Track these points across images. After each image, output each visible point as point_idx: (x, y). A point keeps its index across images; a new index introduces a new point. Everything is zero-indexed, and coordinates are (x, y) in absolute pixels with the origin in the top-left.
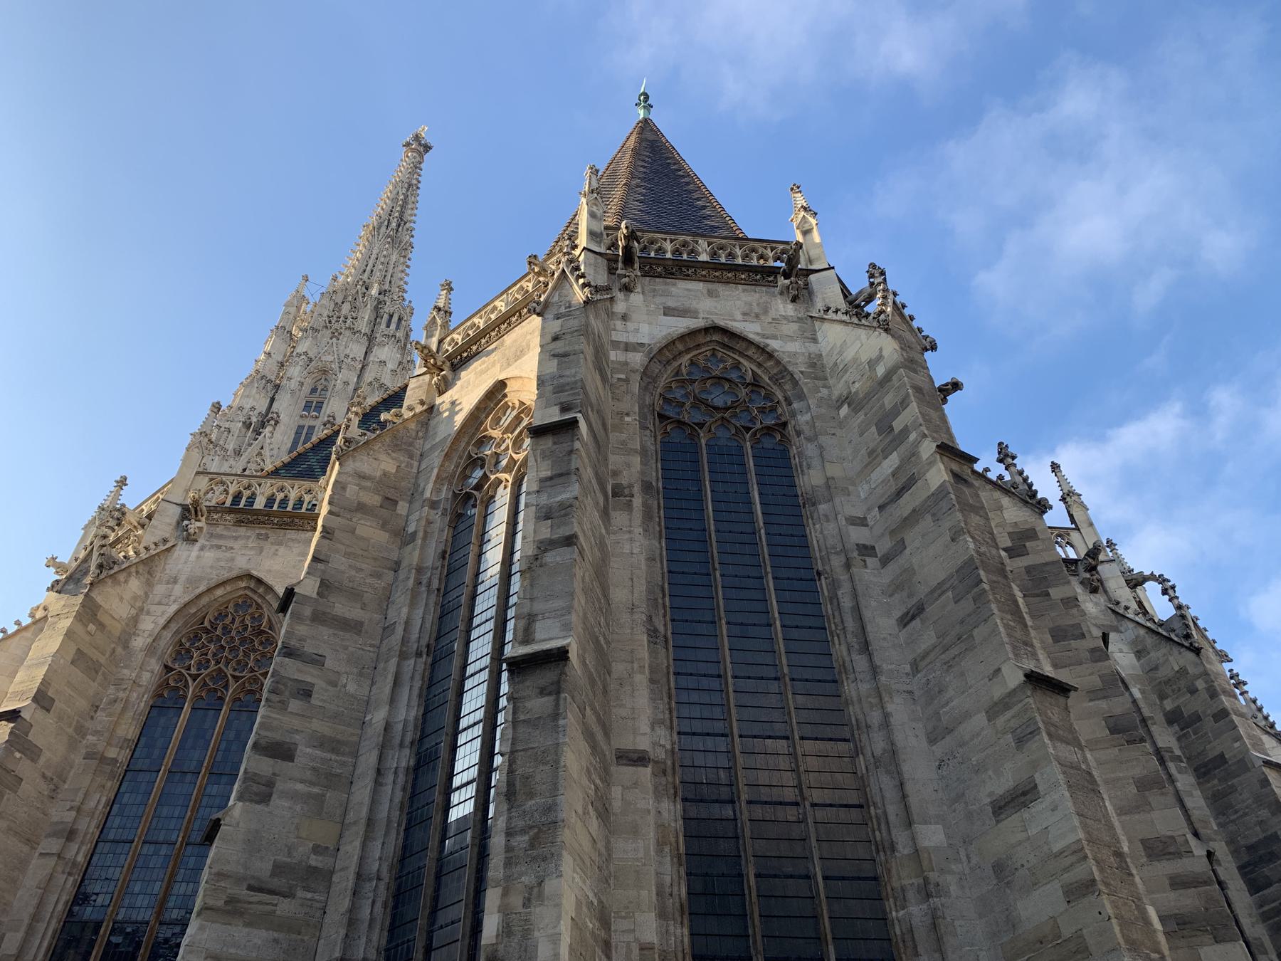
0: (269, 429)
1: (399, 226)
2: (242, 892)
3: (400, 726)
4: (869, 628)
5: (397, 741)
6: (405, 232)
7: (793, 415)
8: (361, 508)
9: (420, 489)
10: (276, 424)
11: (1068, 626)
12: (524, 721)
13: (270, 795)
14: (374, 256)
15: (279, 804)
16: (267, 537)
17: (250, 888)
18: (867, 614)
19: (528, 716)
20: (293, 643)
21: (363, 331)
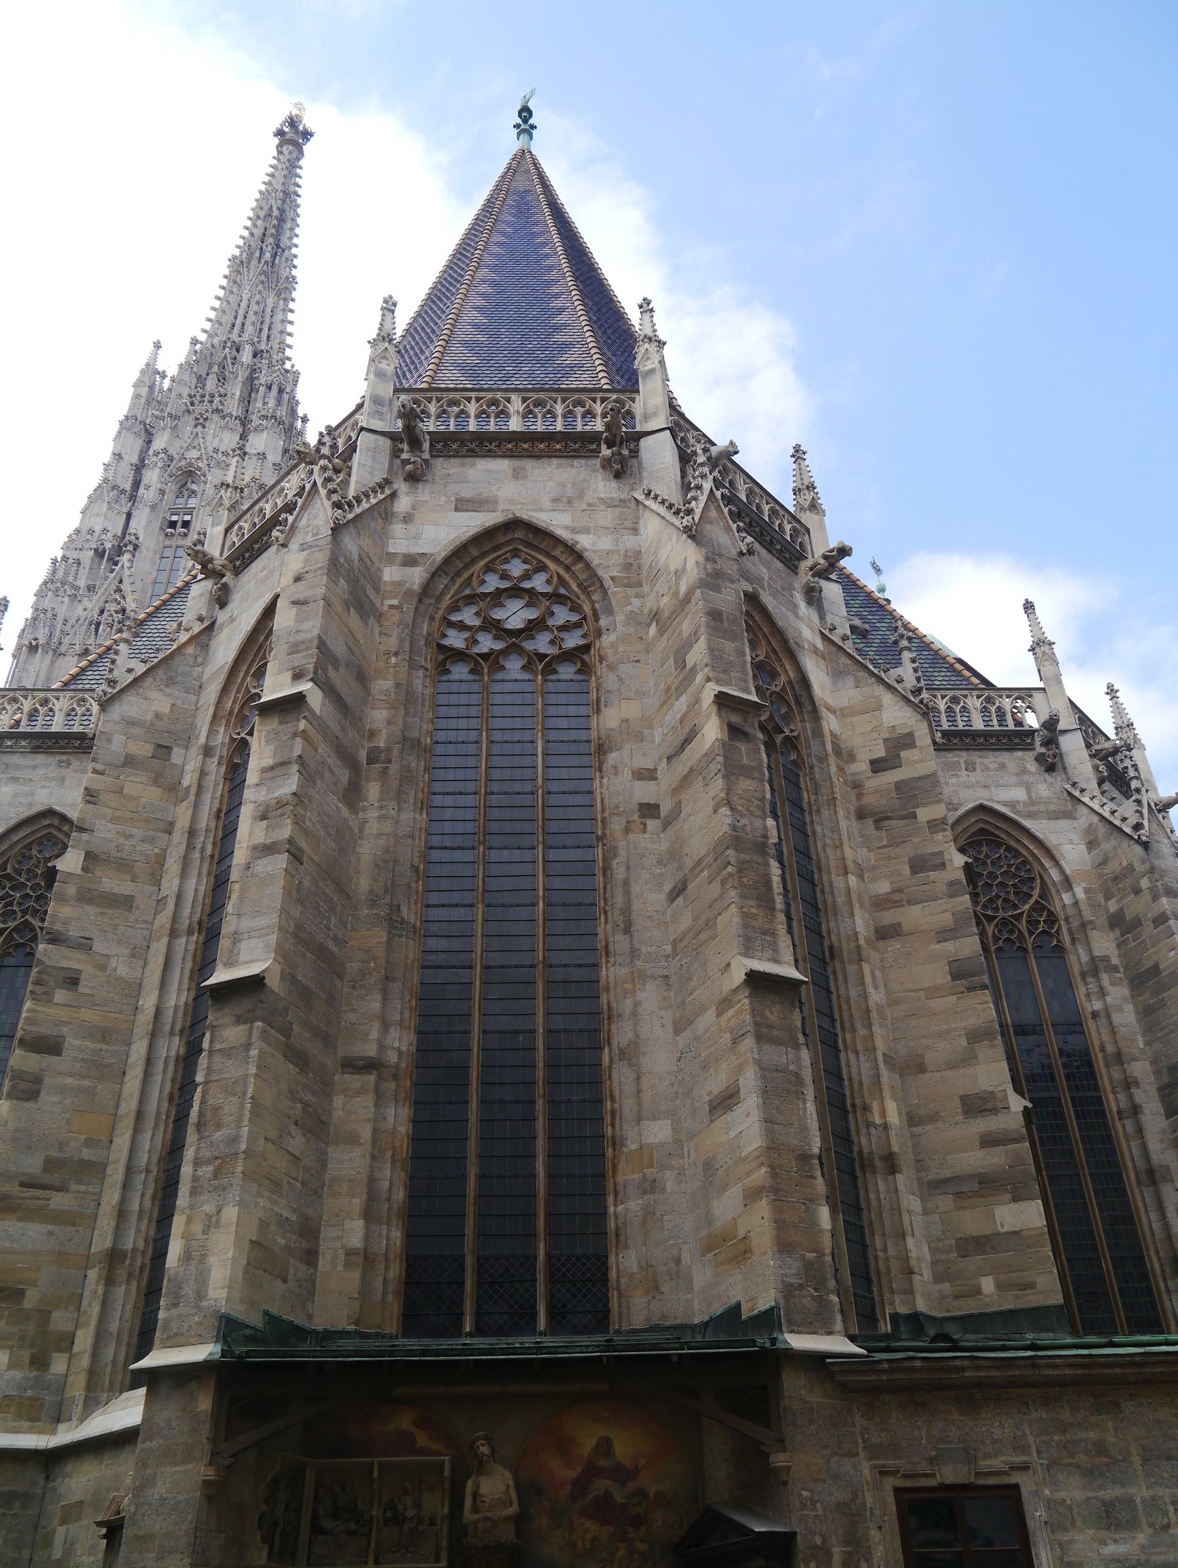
0: (126, 558)
1: (275, 256)
3: (170, 1012)
4: (636, 905)
5: (167, 1028)
6: (284, 265)
7: (599, 633)
8: (130, 761)
9: (197, 732)
10: (135, 549)
11: (930, 854)
12: (219, 1050)
14: (244, 304)
15: (48, 1099)
16: (69, 764)
17: (23, 1184)
18: (636, 888)
19: (223, 1046)
20: (56, 928)
21: (234, 413)
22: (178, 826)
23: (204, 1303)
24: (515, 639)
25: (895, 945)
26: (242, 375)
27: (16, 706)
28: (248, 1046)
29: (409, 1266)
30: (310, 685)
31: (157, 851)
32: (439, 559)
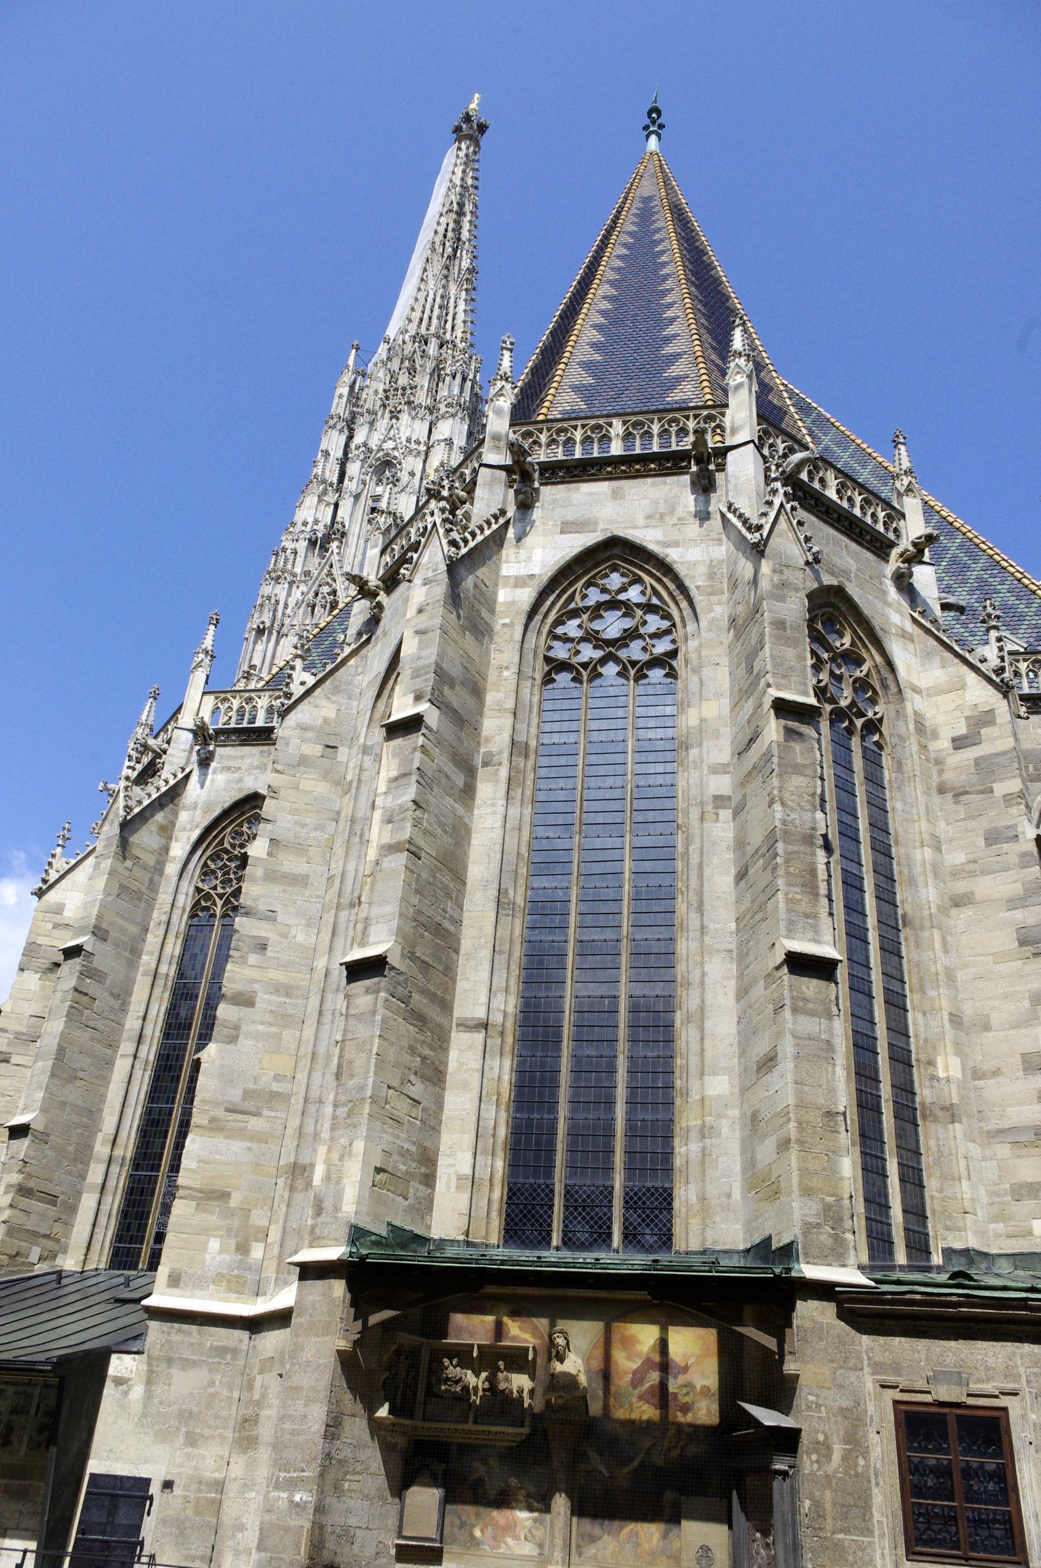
0: (334, 545)
2: (220, 1113)
4: (706, 888)
5: (334, 986)
8: (304, 761)
13: (237, 1037)
17: (227, 1110)
18: (707, 872)
19: (357, 1011)
21: (423, 404)
22: (343, 814)
23: (340, 1215)
24: (611, 648)
25: (965, 914)
26: (430, 365)
27: (227, 705)
28: (374, 1012)
29: (510, 1189)
30: (428, 705)
31: (326, 836)
32: (545, 579)
